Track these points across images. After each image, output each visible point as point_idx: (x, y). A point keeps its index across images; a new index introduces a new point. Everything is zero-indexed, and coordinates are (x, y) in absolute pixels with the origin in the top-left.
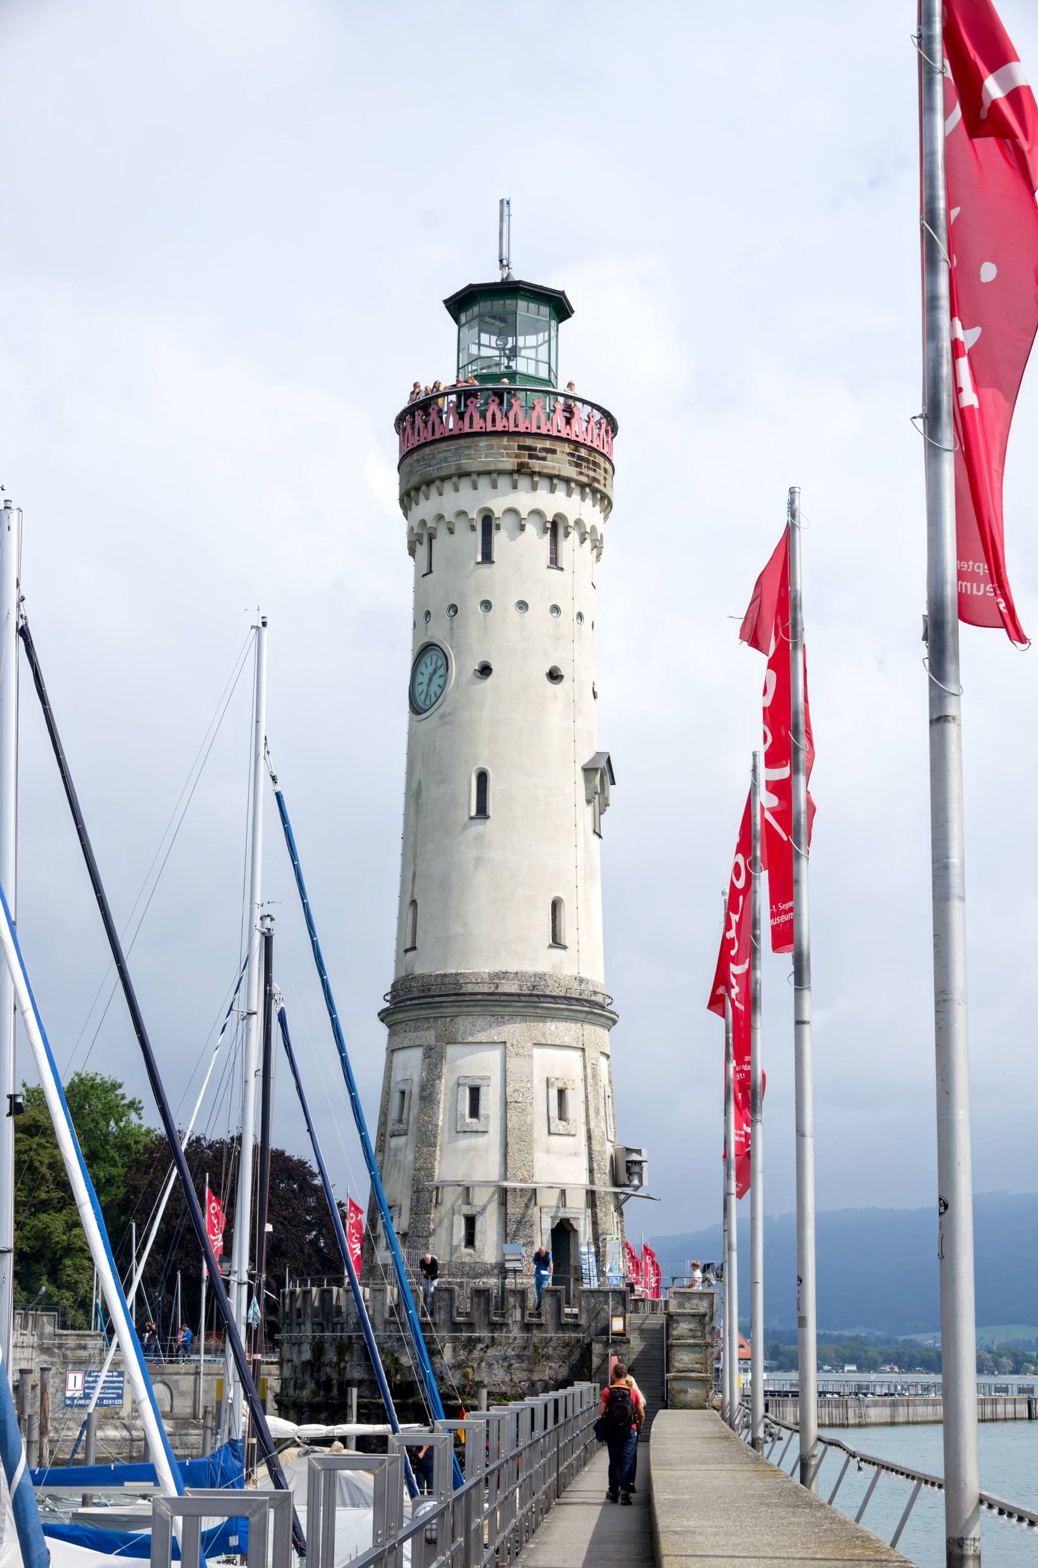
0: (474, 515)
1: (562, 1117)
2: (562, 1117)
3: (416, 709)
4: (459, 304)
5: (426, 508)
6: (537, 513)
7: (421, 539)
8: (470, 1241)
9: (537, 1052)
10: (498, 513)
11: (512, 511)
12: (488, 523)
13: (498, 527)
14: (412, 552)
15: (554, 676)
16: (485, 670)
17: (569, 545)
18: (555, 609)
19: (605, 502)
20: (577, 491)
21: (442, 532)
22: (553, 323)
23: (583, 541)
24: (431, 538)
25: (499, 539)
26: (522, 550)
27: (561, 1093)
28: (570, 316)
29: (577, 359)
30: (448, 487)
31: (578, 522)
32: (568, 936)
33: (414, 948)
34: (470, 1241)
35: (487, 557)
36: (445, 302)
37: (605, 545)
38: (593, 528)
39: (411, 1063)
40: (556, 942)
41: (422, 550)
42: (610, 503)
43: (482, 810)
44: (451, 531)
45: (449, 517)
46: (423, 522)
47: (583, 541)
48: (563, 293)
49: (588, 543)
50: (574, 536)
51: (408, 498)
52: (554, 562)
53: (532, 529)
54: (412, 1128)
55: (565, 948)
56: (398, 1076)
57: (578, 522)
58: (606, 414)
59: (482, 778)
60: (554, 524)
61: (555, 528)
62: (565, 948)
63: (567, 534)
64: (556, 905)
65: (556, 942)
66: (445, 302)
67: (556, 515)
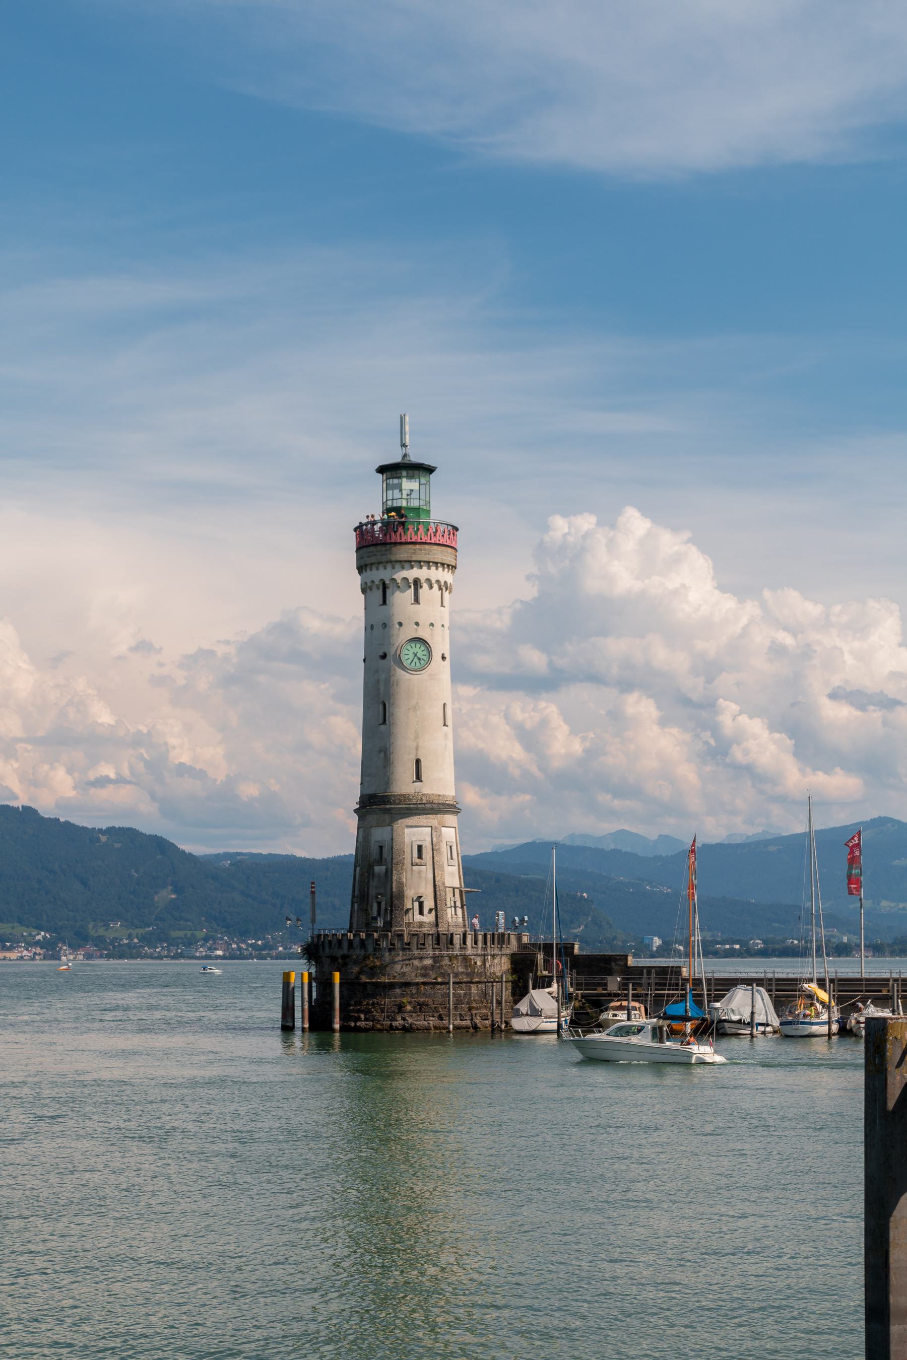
0: (377, 582)
1: (420, 856)
2: (420, 856)
7: (364, 591)
10: (387, 582)
11: (394, 580)
12: (385, 587)
16: (384, 656)
17: (424, 591)
18: (417, 624)
21: (368, 591)
25: (388, 592)
27: (420, 848)
31: (428, 581)
35: (384, 602)
40: (419, 777)
43: (384, 722)
49: (436, 586)
51: (361, 569)
52: (417, 600)
63: (421, 587)
64: (418, 762)
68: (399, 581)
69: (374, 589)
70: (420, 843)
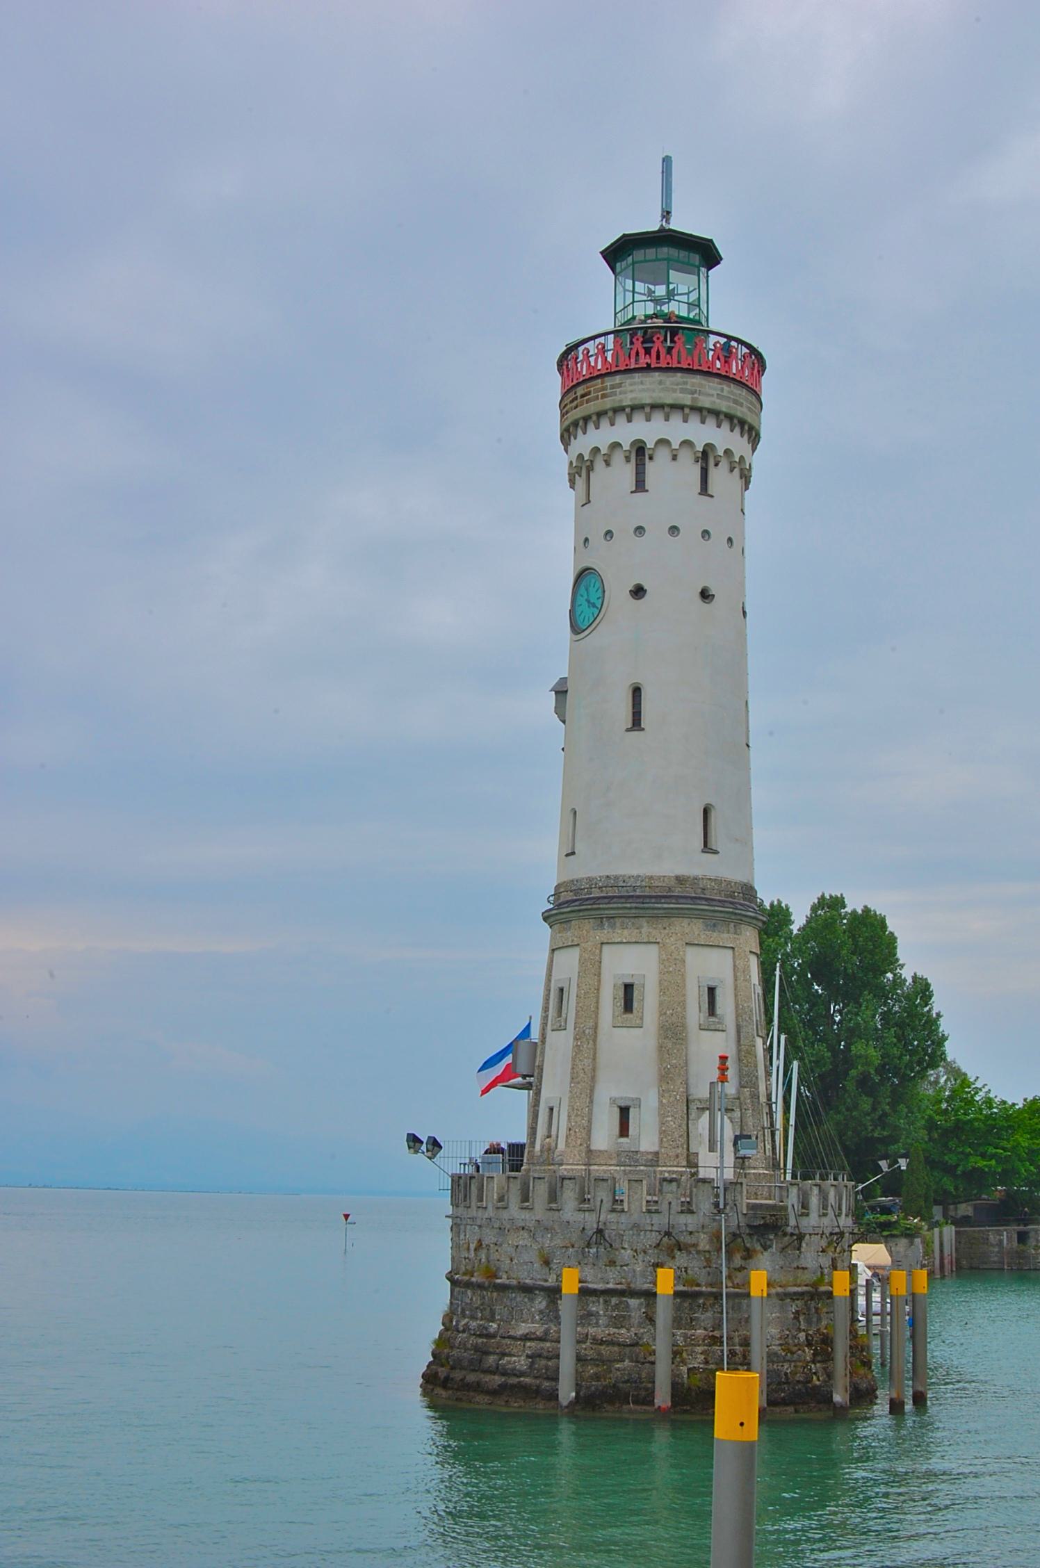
0: (626, 447)
1: (712, 1011)
3: (576, 629)
4: (616, 253)
5: (585, 442)
6: (687, 443)
7: (581, 470)
8: (624, 1130)
9: (690, 950)
10: (650, 445)
13: (651, 458)
14: (572, 487)
15: (705, 595)
16: (638, 592)
18: (706, 534)
19: (753, 435)
20: (726, 426)
21: (599, 464)
22: (703, 270)
23: (732, 470)
24: (590, 469)
25: (650, 467)
26: (672, 479)
27: (711, 991)
28: (718, 263)
29: (727, 304)
30: (604, 423)
32: (717, 841)
33: (573, 853)
34: (624, 1130)
35: (640, 486)
36: (602, 253)
37: (753, 473)
38: (742, 458)
39: (569, 961)
41: (580, 482)
42: (758, 435)
44: (608, 463)
45: (604, 450)
46: (580, 456)
47: (732, 470)
48: (711, 241)
49: (737, 471)
50: (724, 465)
51: (567, 435)
52: (704, 489)
53: (686, 457)
54: (571, 1025)
55: (716, 852)
56: (559, 976)
57: (728, 452)
58: (753, 351)
59: (637, 691)
60: (705, 454)
61: (705, 457)
62: (716, 852)
63: (716, 465)
64: (706, 812)
65: (707, 847)
66: (602, 253)
67: (706, 445)
68: (675, 446)
69: (618, 458)
70: (712, 984)
